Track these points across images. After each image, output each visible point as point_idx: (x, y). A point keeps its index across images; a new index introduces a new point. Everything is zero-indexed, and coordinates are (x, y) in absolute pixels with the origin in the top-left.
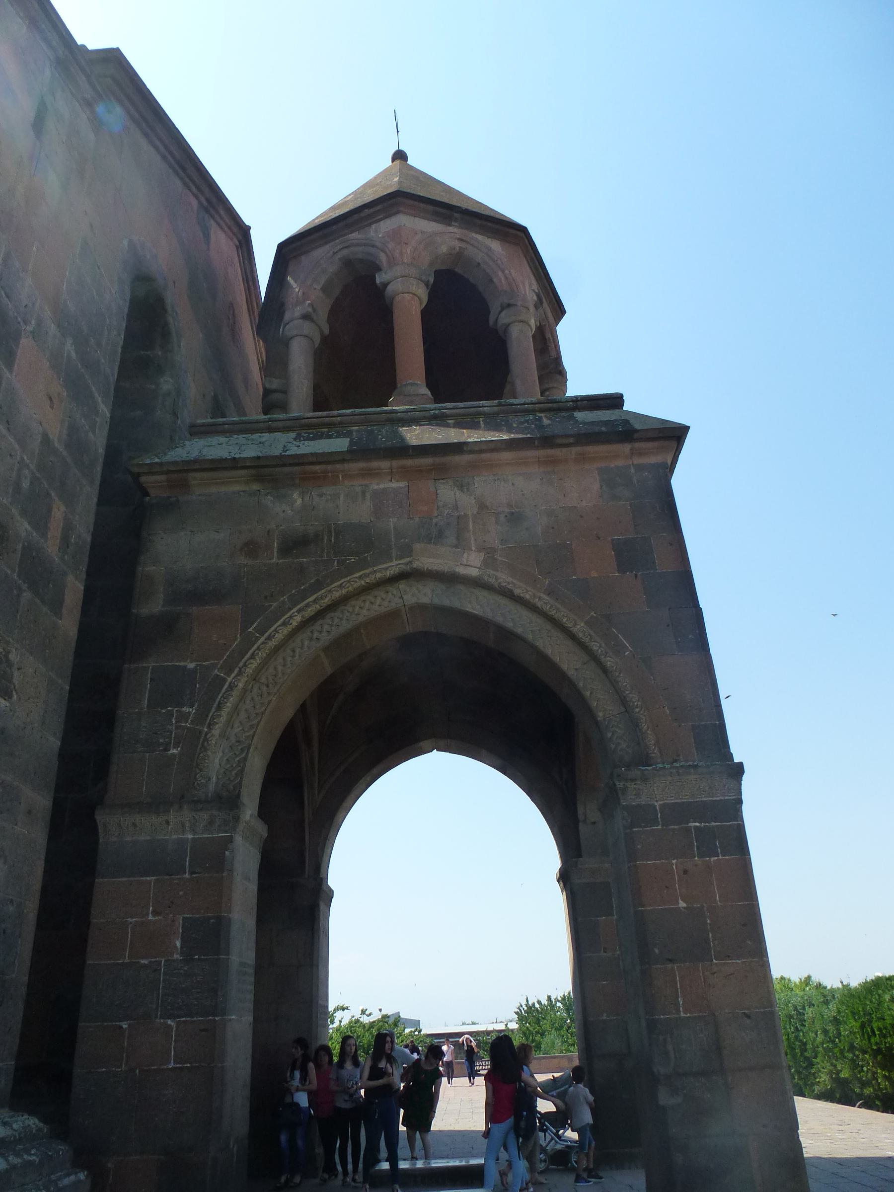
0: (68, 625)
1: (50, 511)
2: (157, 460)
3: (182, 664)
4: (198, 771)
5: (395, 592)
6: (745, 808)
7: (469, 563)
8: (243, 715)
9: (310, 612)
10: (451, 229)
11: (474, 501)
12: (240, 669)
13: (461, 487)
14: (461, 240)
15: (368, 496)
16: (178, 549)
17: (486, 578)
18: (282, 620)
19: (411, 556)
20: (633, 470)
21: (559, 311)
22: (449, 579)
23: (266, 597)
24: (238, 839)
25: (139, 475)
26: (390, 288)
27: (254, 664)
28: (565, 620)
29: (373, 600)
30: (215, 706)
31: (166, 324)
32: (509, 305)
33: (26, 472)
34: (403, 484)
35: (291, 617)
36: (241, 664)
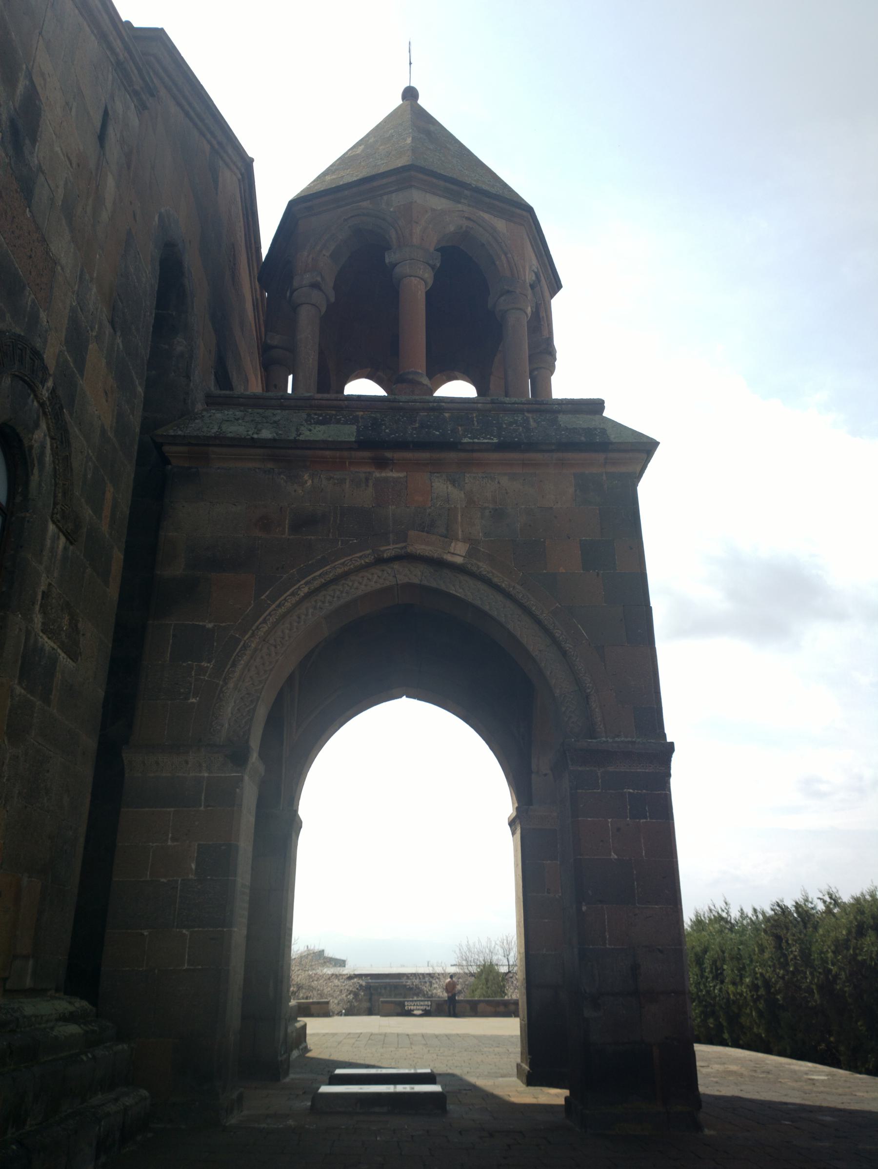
0: (113, 592)
2: (180, 433)
5: (390, 571)
6: (673, 781)
9: (316, 584)
10: (460, 207)
11: (463, 496)
12: (254, 631)
13: (453, 482)
14: (468, 219)
15: (371, 483)
16: (199, 518)
17: (469, 566)
19: (405, 541)
20: (604, 478)
21: (556, 285)
22: (438, 564)
24: (246, 778)
26: (398, 270)
27: (265, 628)
28: (534, 608)
29: (370, 577)
30: (230, 663)
32: (508, 292)
33: (90, 464)
35: (299, 588)
36: (254, 628)
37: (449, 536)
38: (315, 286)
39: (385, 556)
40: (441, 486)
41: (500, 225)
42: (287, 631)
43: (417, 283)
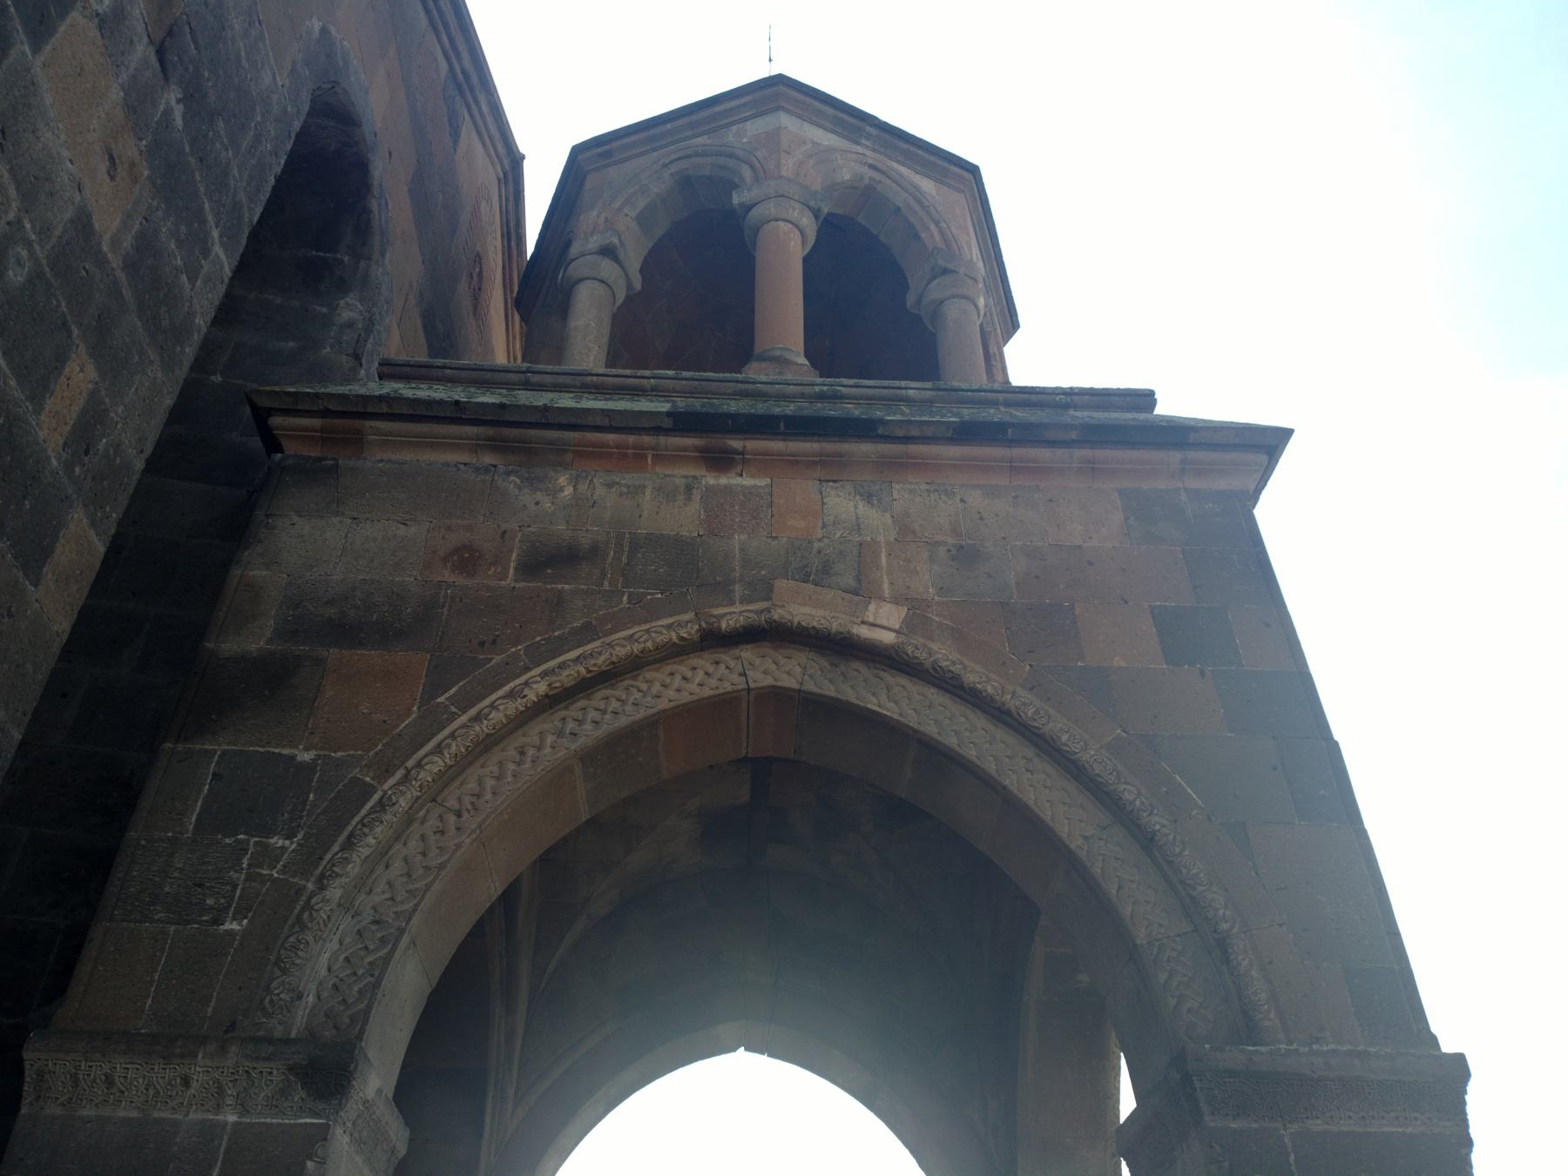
1: (61, 359)
3: (286, 751)
4: (277, 973)
5: (732, 663)
7: (878, 622)
8: (398, 867)
9: (567, 678)
10: (859, 149)
11: (890, 521)
12: (408, 771)
13: (868, 498)
14: (871, 167)
15: (697, 496)
16: (319, 546)
17: (910, 649)
18: (507, 688)
19: (769, 599)
20: (1184, 497)
22: (839, 647)
23: (482, 644)
24: (341, 1139)
25: (270, 412)
26: (754, 212)
27: (437, 765)
28: (1064, 738)
29: (689, 674)
30: (341, 839)
31: (367, 211)
32: (945, 271)
34: (763, 482)
35: (526, 684)
36: (410, 764)
37: (862, 591)
38: (608, 252)
39: (724, 626)
40: (842, 503)
41: (927, 185)
42: (490, 782)
43: (786, 248)
